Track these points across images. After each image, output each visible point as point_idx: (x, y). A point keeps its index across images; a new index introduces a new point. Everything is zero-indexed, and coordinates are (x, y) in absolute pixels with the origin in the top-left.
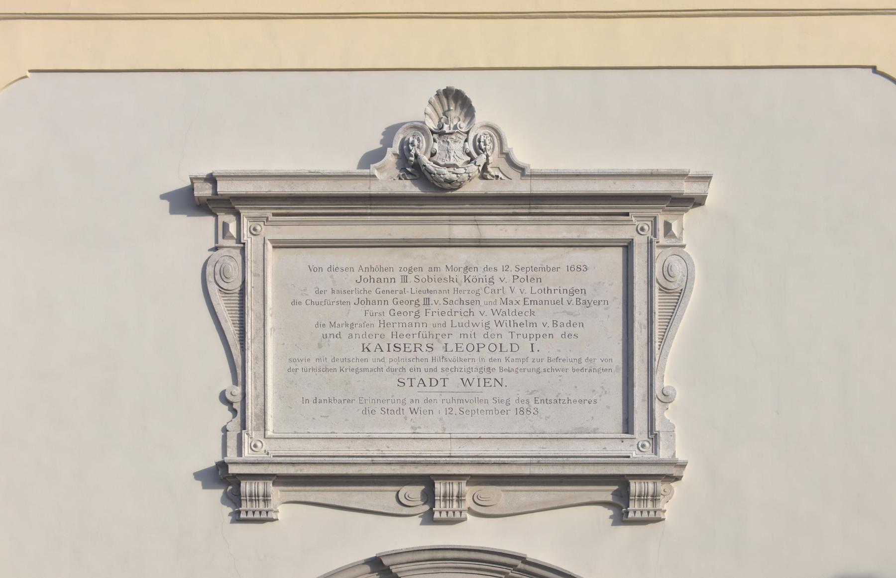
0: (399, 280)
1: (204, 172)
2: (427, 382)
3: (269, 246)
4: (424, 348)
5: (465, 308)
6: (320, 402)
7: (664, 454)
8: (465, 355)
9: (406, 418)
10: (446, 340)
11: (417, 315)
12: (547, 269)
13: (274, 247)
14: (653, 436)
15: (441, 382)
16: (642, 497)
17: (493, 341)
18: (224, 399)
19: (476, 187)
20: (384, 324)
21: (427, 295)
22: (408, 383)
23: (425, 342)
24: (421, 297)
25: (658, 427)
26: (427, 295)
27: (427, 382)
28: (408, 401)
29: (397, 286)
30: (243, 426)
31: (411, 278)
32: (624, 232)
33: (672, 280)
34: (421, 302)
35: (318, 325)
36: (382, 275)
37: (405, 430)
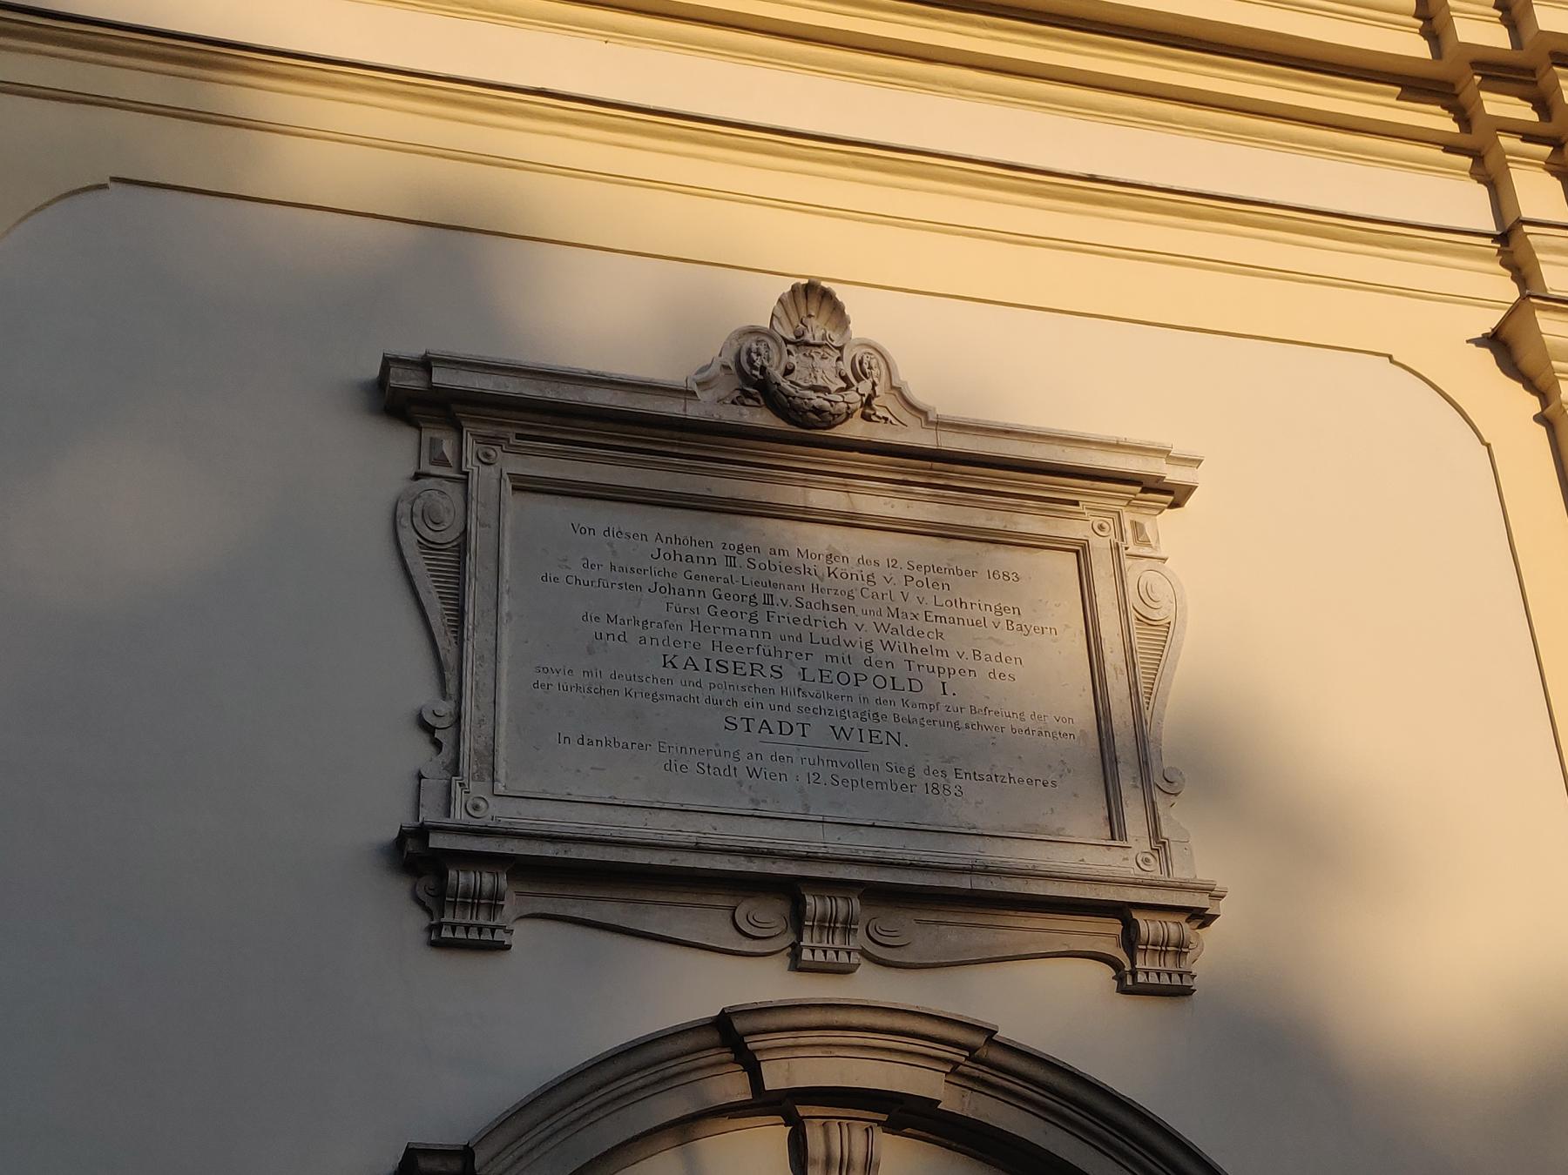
0: (722, 562)
1: (415, 350)
2: (775, 727)
3: (508, 485)
4: (767, 671)
5: (831, 616)
6: (590, 743)
8: (835, 689)
9: (740, 783)
10: (802, 663)
11: (753, 618)
12: (958, 572)
13: (514, 488)
15: (798, 730)
17: (879, 671)
20: (699, 627)
21: (769, 590)
22: (742, 725)
23: (768, 662)
24: (760, 592)
25: (1165, 832)
26: (769, 590)
27: (775, 727)
28: (743, 755)
29: (720, 570)
31: (741, 560)
33: (1155, 605)
34: (760, 599)
35: (585, 617)
36: (694, 551)
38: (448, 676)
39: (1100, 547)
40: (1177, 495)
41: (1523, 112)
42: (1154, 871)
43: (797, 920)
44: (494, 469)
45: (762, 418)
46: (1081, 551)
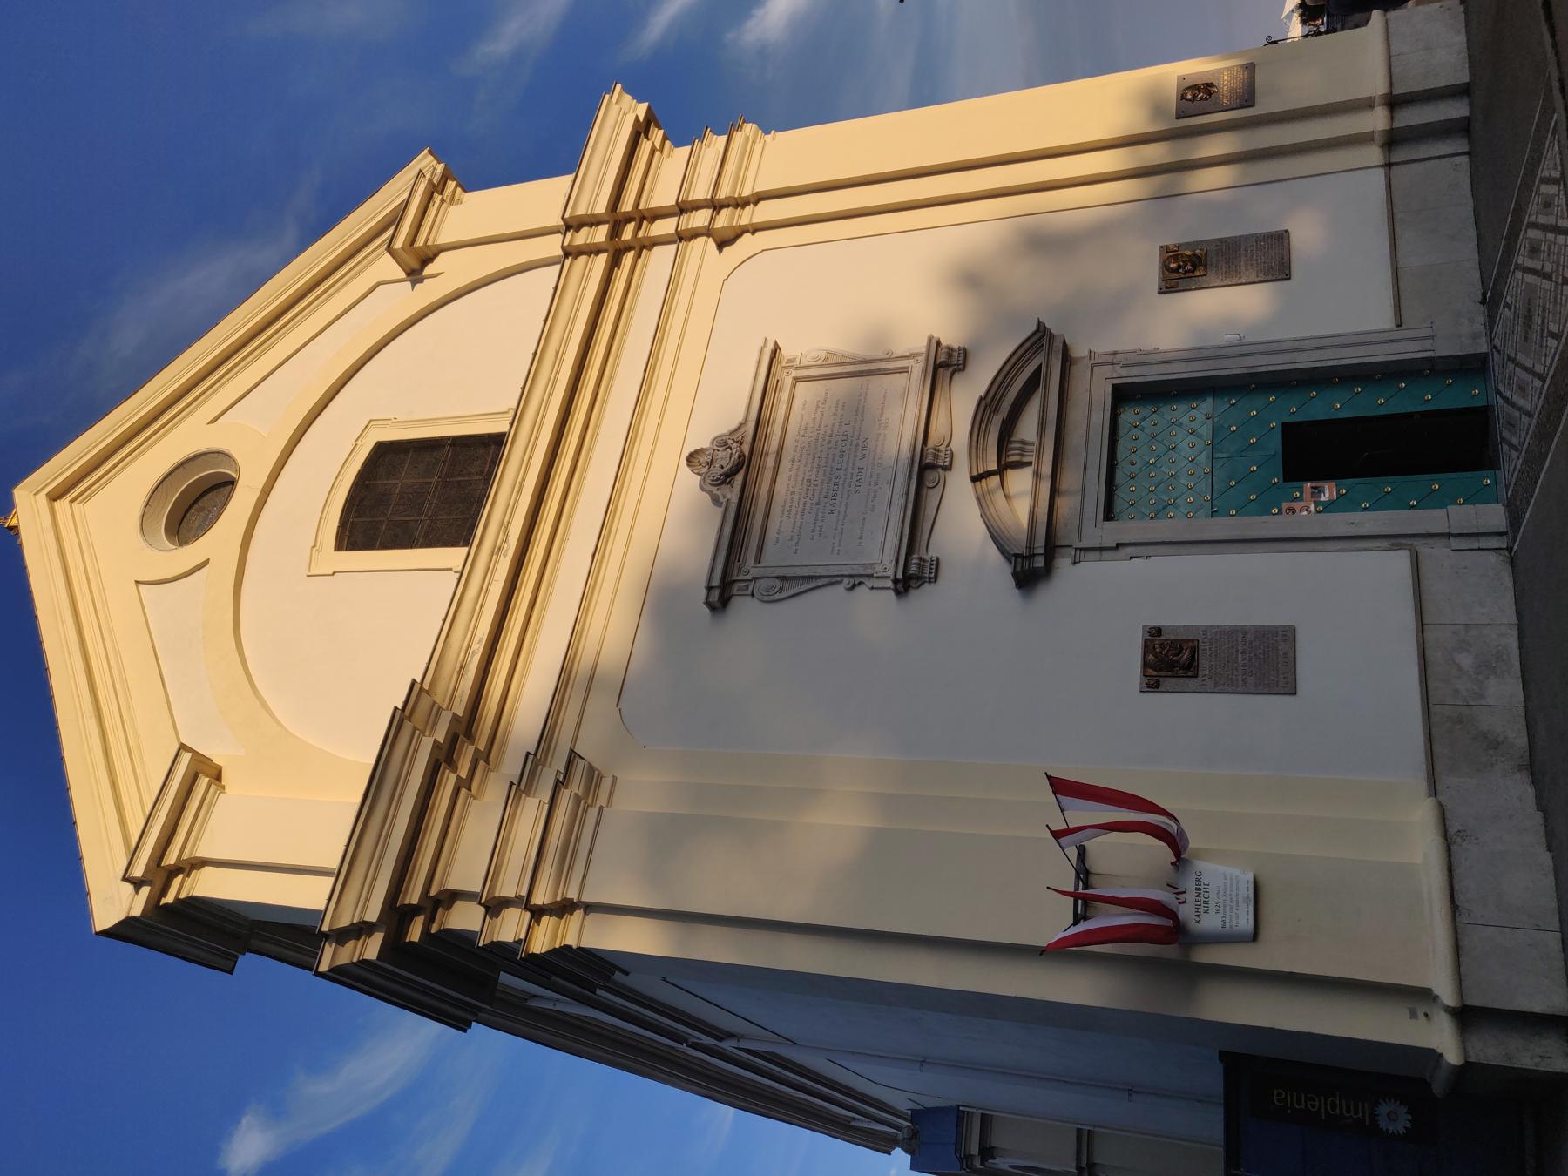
14: (911, 356)
19: (746, 448)
29: (796, 497)
30: (870, 576)
37: (888, 488)
38: (833, 580)
39: (794, 374)
40: (776, 350)
41: (630, 227)
42: (922, 358)
43: (933, 467)
45: (739, 478)
46: (797, 380)
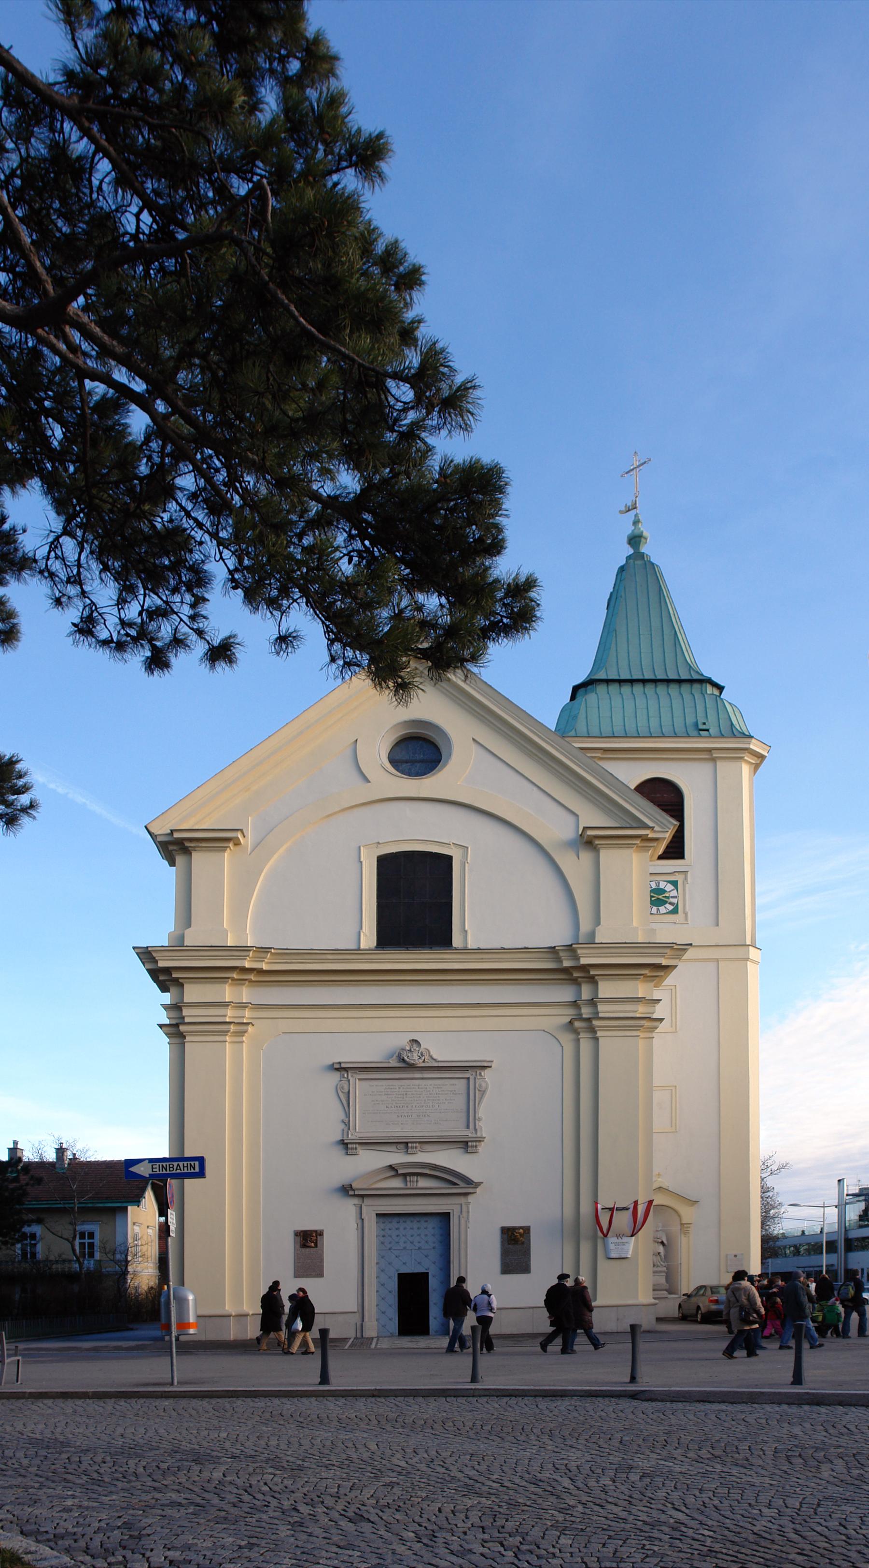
7: (479, 1135)
16: (472, 1146)
18: (343, 1121)
32: (467, 1075)
44: (353, 1078)
